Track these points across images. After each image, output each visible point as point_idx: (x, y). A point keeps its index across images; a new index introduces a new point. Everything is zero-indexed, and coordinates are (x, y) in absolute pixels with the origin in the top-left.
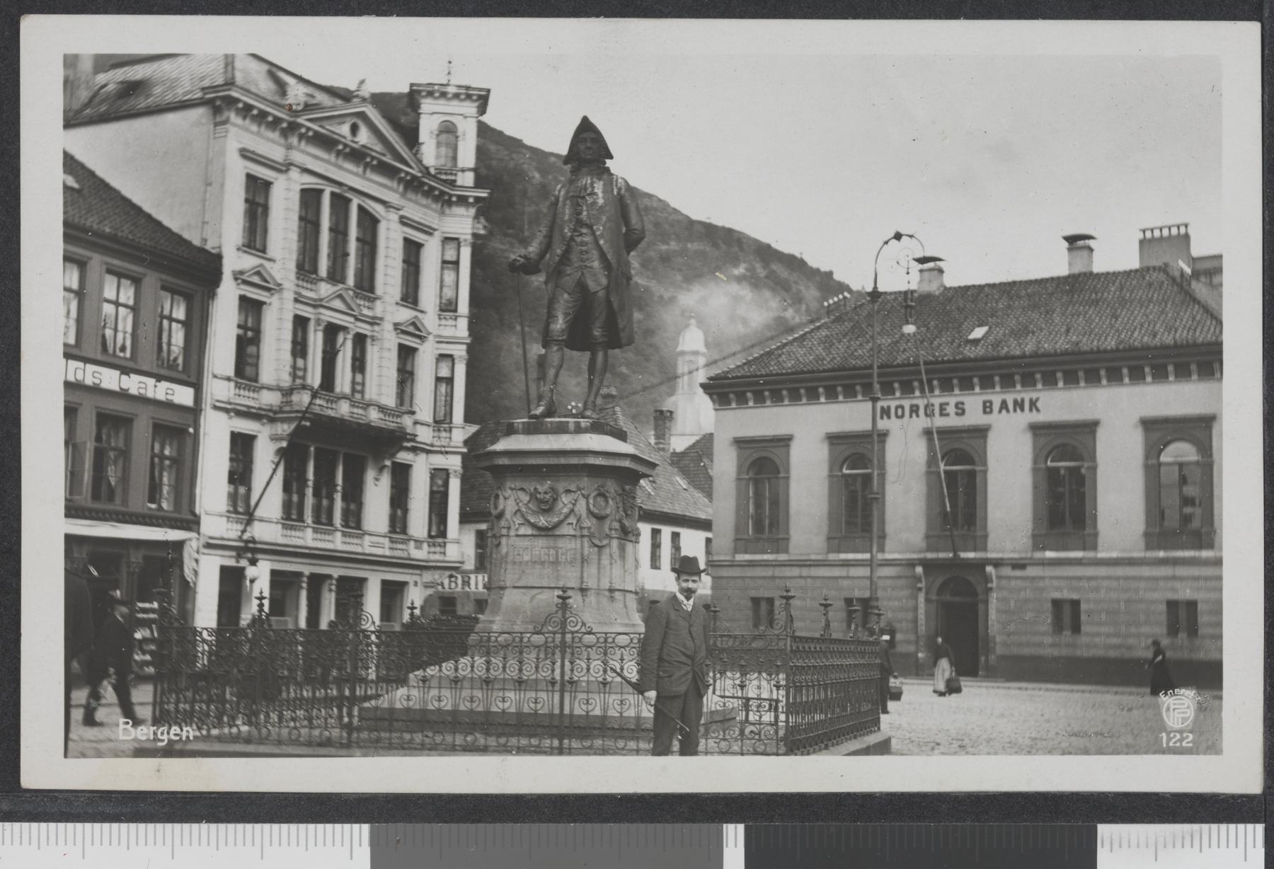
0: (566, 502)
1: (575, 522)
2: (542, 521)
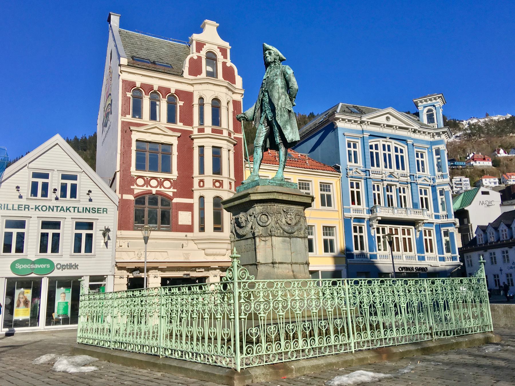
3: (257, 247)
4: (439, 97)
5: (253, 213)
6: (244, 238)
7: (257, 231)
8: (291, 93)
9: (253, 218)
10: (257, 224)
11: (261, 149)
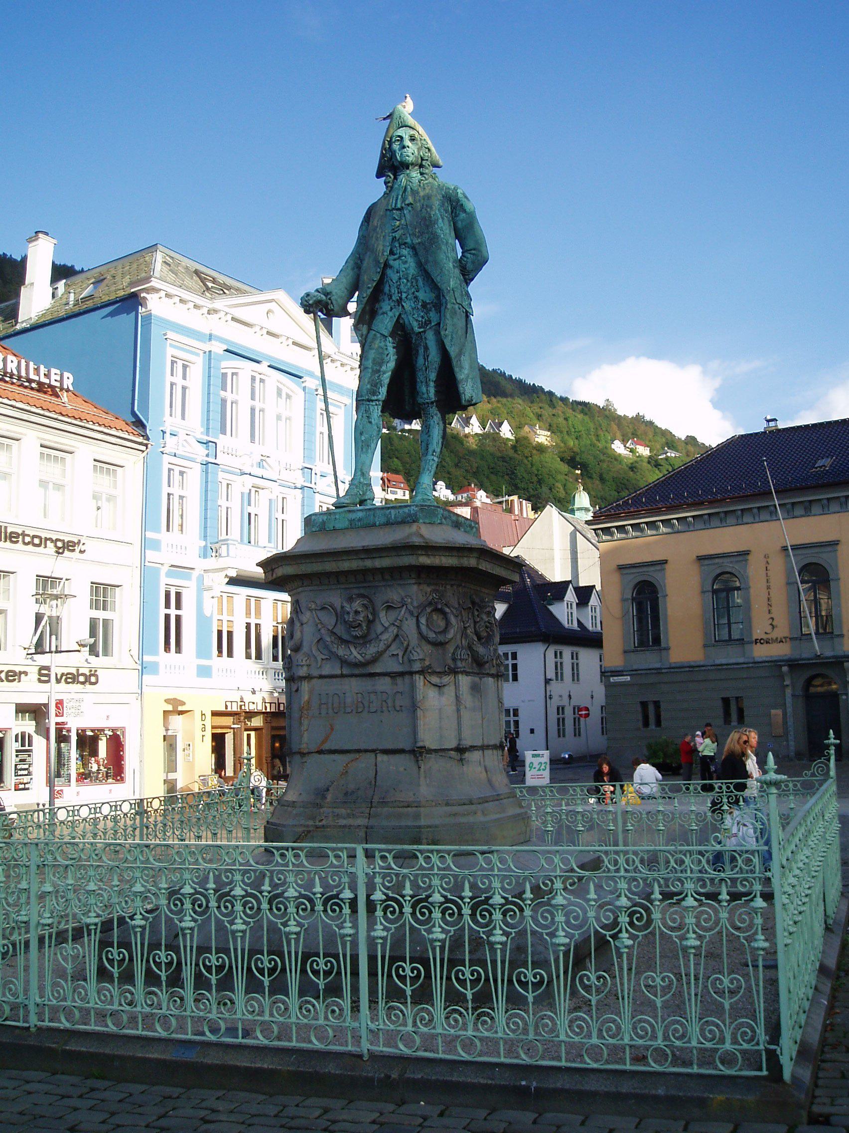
0: (386, 625)
1: (401, 654)
2: (355, 654)
11: (380, 408)
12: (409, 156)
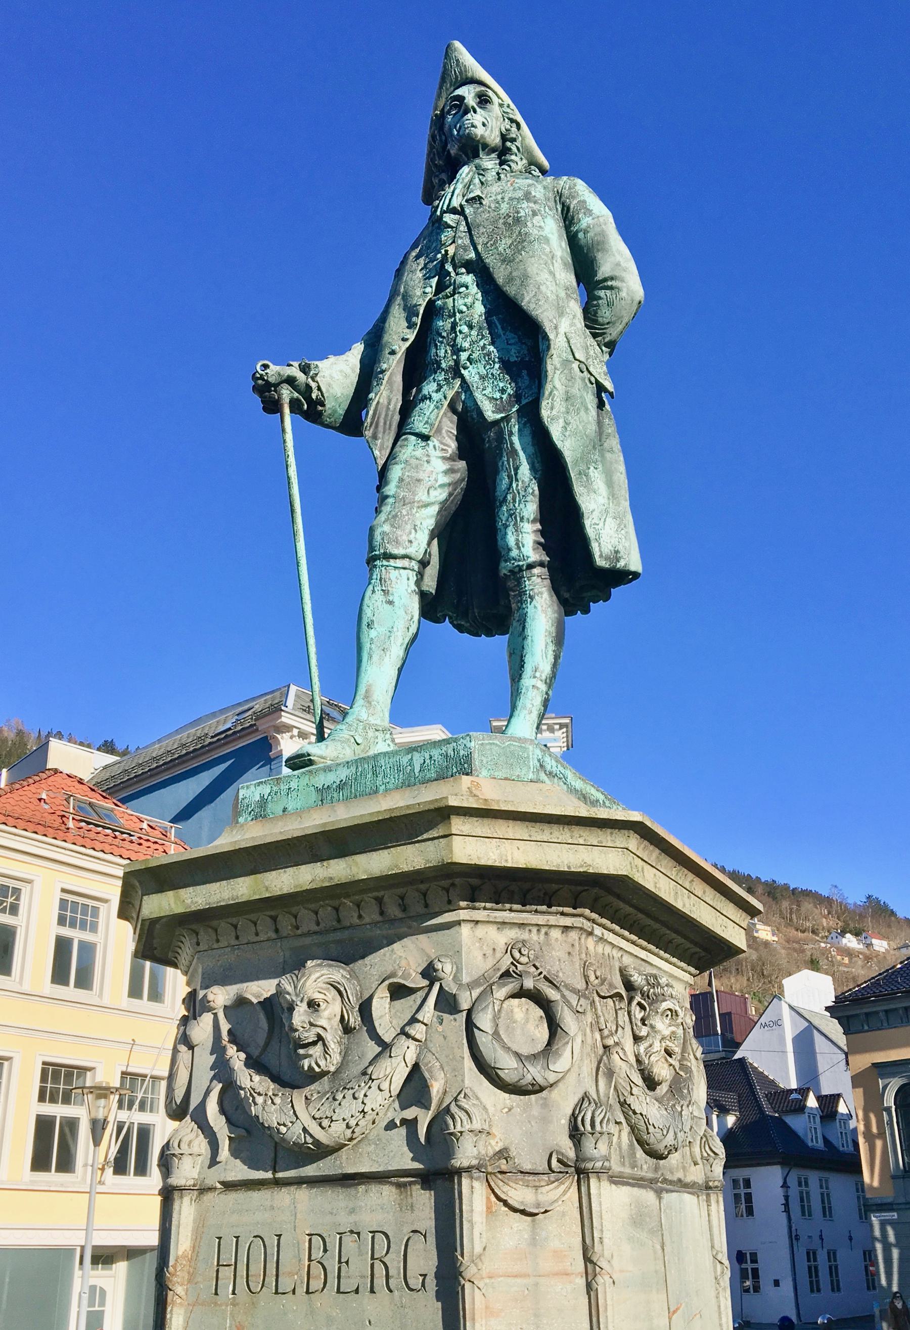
3: (469, 1270)
4: (562, 726)
5: (430, 973)
6: (310, 1170)
7: (477, 1125)
8: (605, 314)
9: (429, 1012)
10: (469, 1063)
12: (475, 127)
